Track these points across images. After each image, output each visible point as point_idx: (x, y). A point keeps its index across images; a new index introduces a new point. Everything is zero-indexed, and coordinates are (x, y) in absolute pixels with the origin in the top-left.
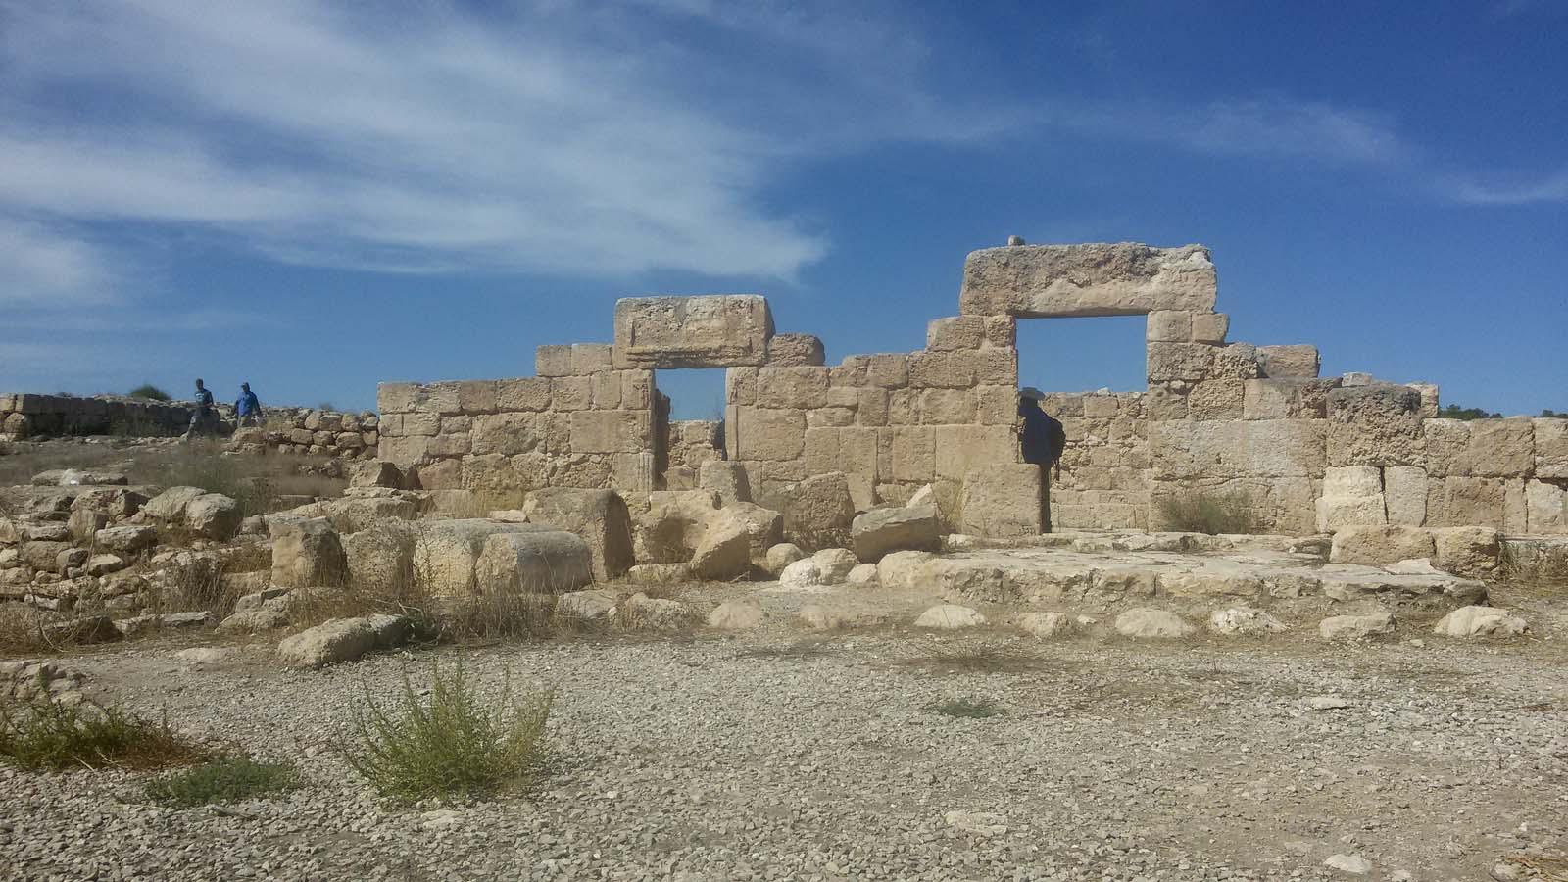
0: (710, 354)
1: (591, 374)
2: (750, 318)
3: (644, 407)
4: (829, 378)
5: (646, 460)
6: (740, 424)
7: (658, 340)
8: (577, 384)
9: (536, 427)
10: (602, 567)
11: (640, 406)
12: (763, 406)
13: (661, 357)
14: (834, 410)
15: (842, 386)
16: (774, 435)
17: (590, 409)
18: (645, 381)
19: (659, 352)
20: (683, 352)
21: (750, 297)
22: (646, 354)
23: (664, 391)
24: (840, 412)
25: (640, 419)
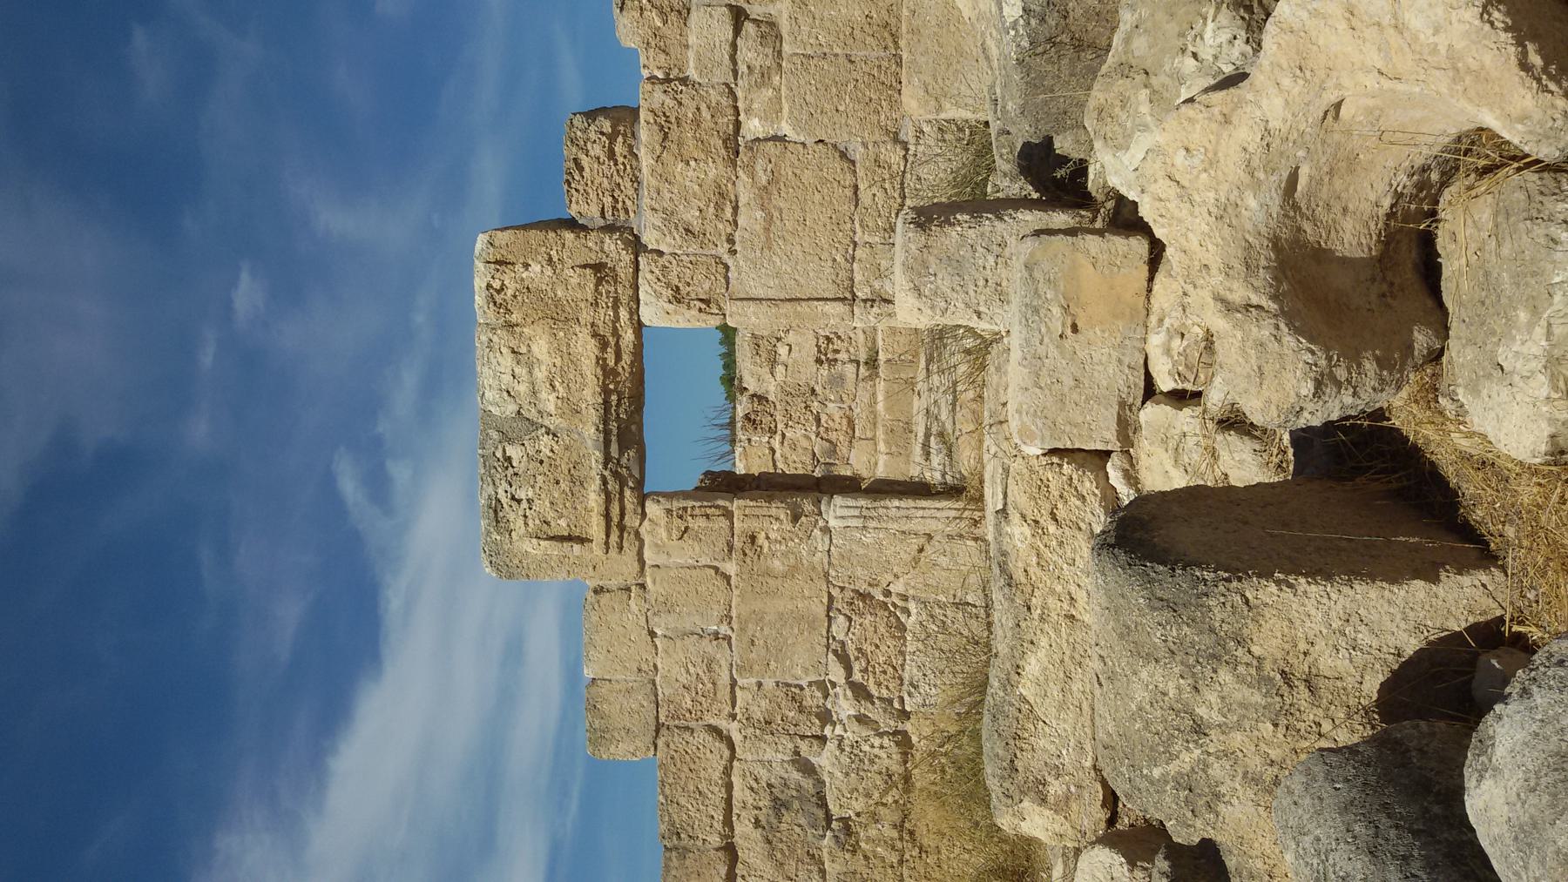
0: (611, 363)
1: (652, 634)
2: (526, 266)
3: (728, 515)
4: (668, 80)
5: (846, 512)
6: (771, 294)
7: (578, 482)
8: (673, 668)
9: (767, 759)
10: (1439, 590)
11: (723, 523)
12: (731, 241)
13: (616, 474)
14: (742, 68)
15: (687, 46)
16: (798, 214)
17: (728, 639)
18: (669, 512)
19: (605, 482)
20: (605, 422)
21: (479, 265)
22: (607, 509)
23: (692, 481)
24: (750, 53)
25: (754, 525)
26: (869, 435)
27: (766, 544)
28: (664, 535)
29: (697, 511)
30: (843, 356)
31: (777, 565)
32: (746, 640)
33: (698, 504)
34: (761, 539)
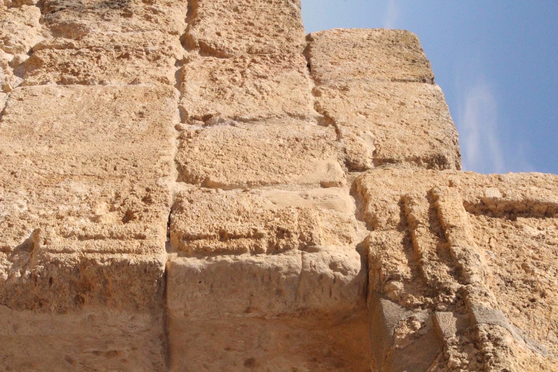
1: (326, 120)
3: (178, 241)
11: (187, 226)
13: (434, 289)
18: (308, 246)
19: (459, 273)
27: (101, 209)
28: (314, 214)
29: (246, 243)
31: (80, 187)
32: (155, 116)
33: (244, 257)
34: (110, 220)
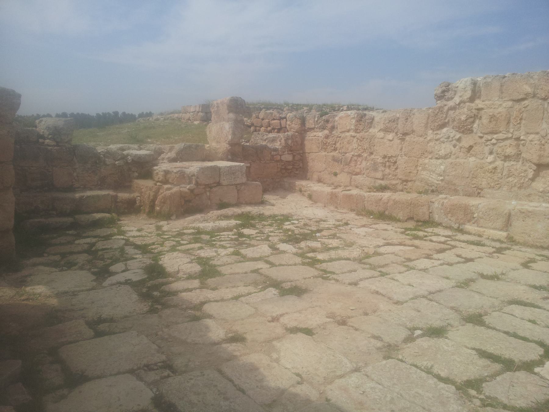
26: (353, 183)
30: (387, 171)
